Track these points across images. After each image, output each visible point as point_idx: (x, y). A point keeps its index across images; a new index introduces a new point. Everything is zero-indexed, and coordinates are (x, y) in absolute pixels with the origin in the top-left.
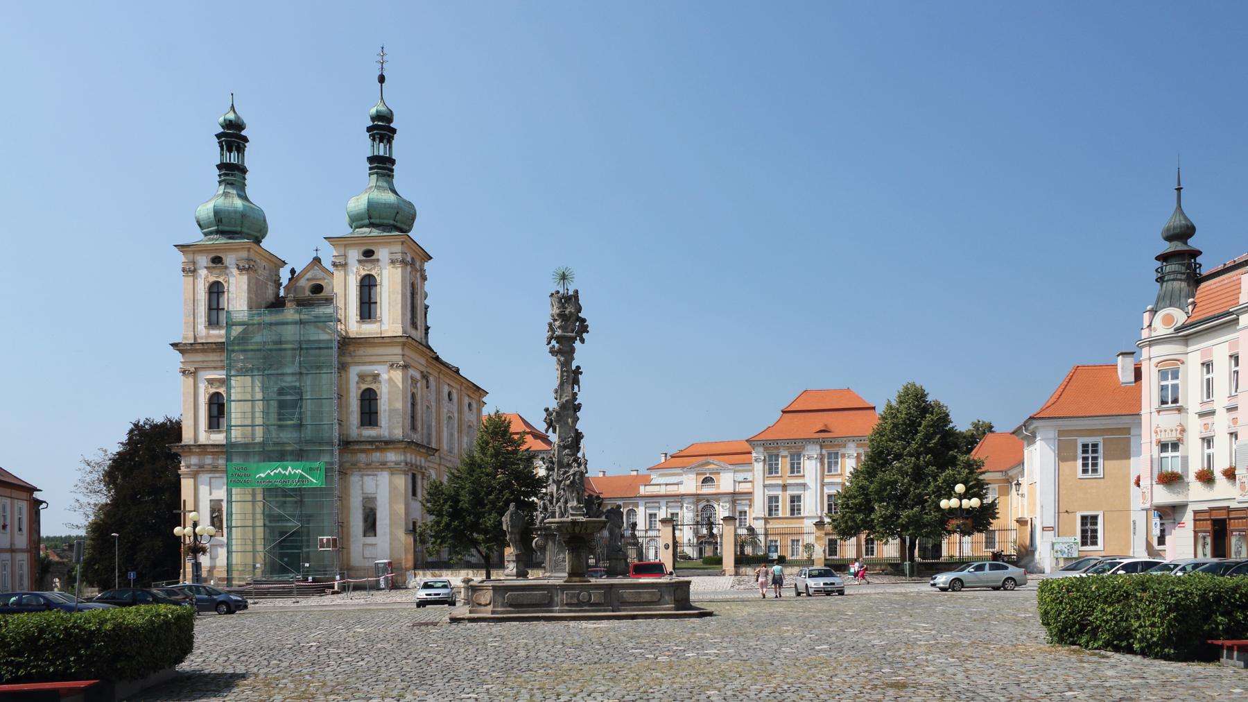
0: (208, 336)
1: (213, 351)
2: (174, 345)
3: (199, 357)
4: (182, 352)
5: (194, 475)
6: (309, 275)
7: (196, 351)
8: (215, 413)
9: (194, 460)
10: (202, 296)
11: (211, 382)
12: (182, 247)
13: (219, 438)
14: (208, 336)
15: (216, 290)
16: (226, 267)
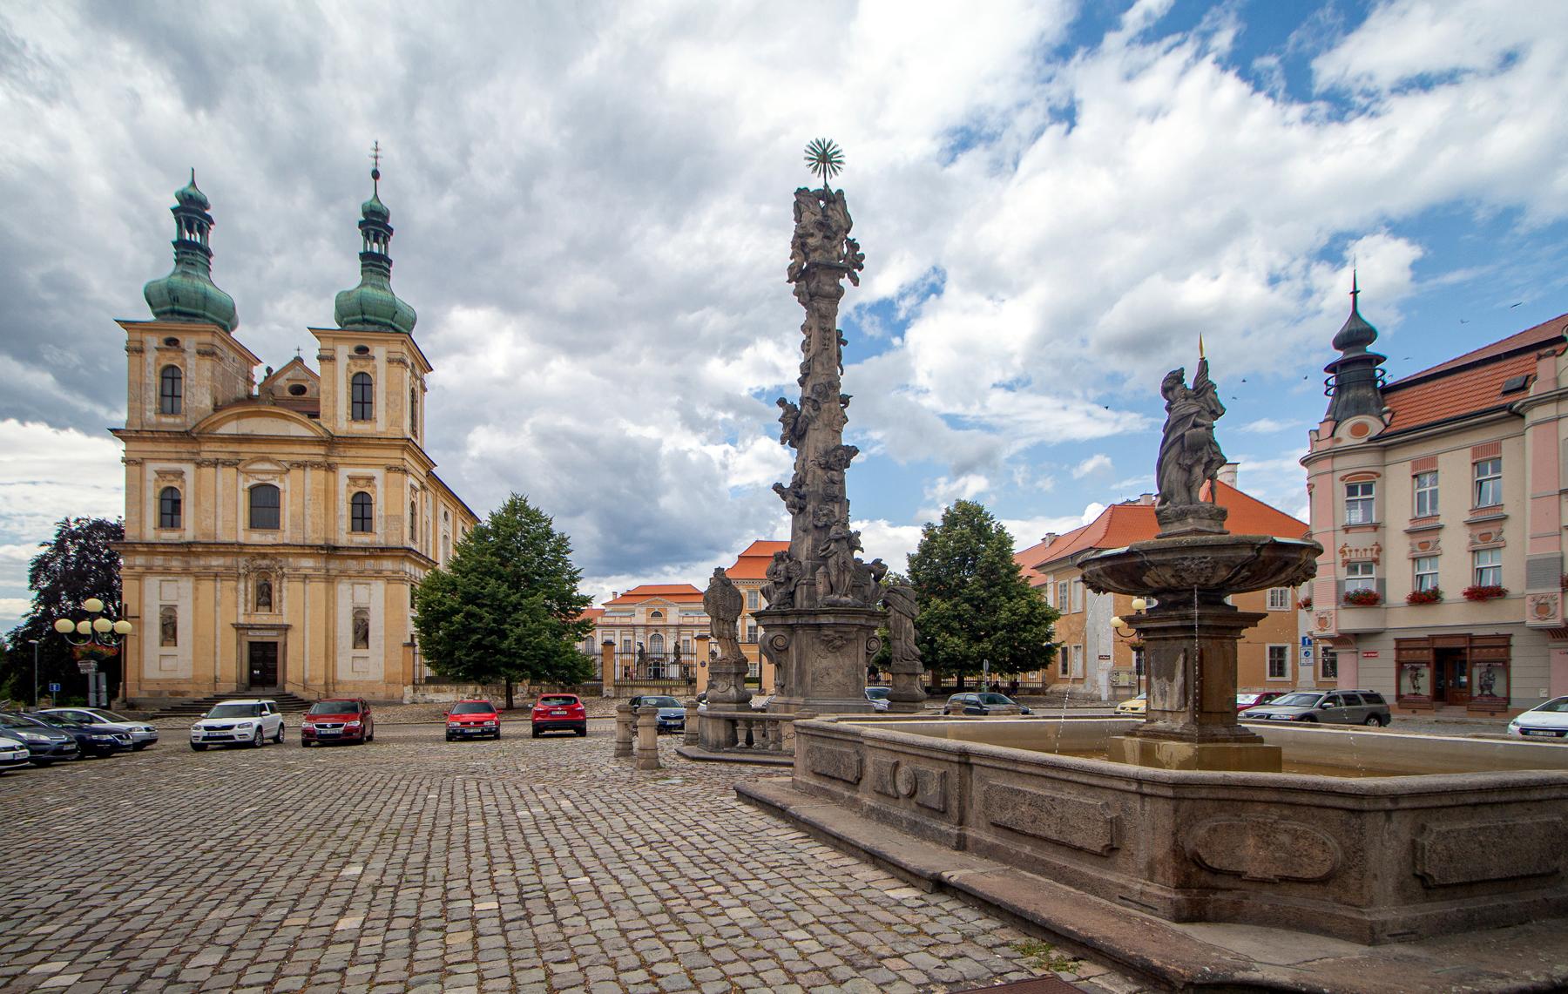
0: (161, 424)
1: (167, 440)
4: (124, 439)
5: (139, 577)
7: (144, 439)
8: (168, 509)
9: (140, 560)
10: (153, 379)
11: (161, 474)
12: (127, 324)
13: (169, 536)
15: (171, 377)
16: (183, 351)
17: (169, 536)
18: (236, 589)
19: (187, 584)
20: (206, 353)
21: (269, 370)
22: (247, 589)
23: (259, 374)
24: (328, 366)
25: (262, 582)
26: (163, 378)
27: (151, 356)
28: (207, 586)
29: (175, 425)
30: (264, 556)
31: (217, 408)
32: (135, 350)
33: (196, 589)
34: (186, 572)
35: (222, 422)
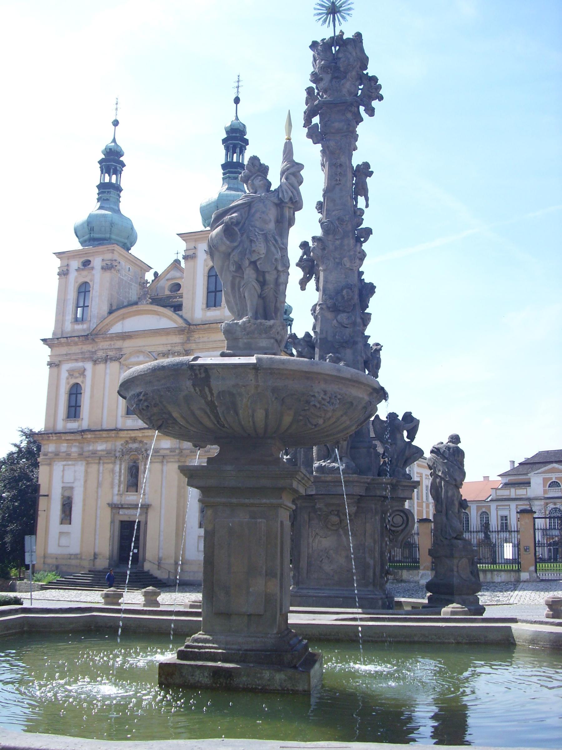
2: (42, 340)
3: (63, 350)
6: (168, 276)
10: (72, 295)
14: (73, 331)
15: (84, 290)
17: (73, 425)
18: (113, 471)
19: (80, 467)
20: (108, 267)
21: (156, 274)
22: (120, 470)
23: (149, 277)
24: (191, 263)
25: (131, 464)
26: (79, 293)
27: (73, 275)
28: (94, 468)
29: (84, 330)
30: (134, 440)
31: (111, 312)
32: (63, 273)
33: (86, 472)
34: (81, 456)
35: (111, 324)
